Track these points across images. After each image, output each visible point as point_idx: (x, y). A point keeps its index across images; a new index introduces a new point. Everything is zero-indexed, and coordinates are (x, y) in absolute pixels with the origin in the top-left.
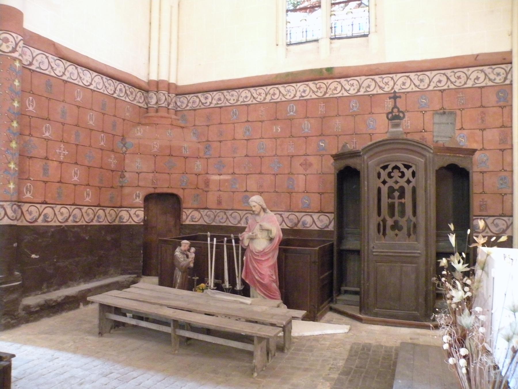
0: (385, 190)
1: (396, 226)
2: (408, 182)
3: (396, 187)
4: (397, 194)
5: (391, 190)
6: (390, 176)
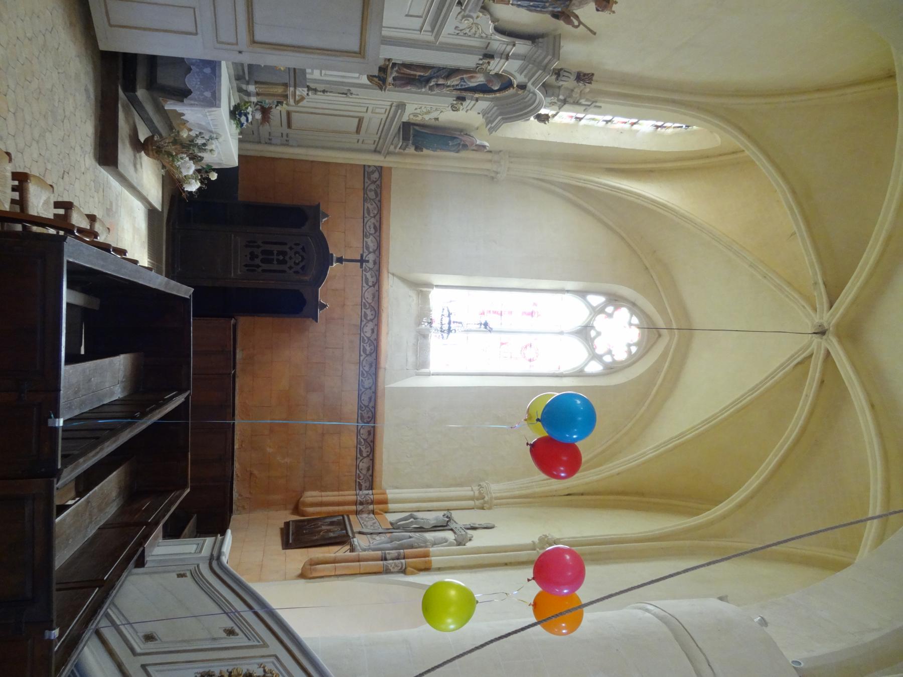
0: (286, 248)
1: (253, 256)
2: (290, 268)
3: (287, 258)
4: (281, 258)
5: (284, 253)
6: (296, 253)
